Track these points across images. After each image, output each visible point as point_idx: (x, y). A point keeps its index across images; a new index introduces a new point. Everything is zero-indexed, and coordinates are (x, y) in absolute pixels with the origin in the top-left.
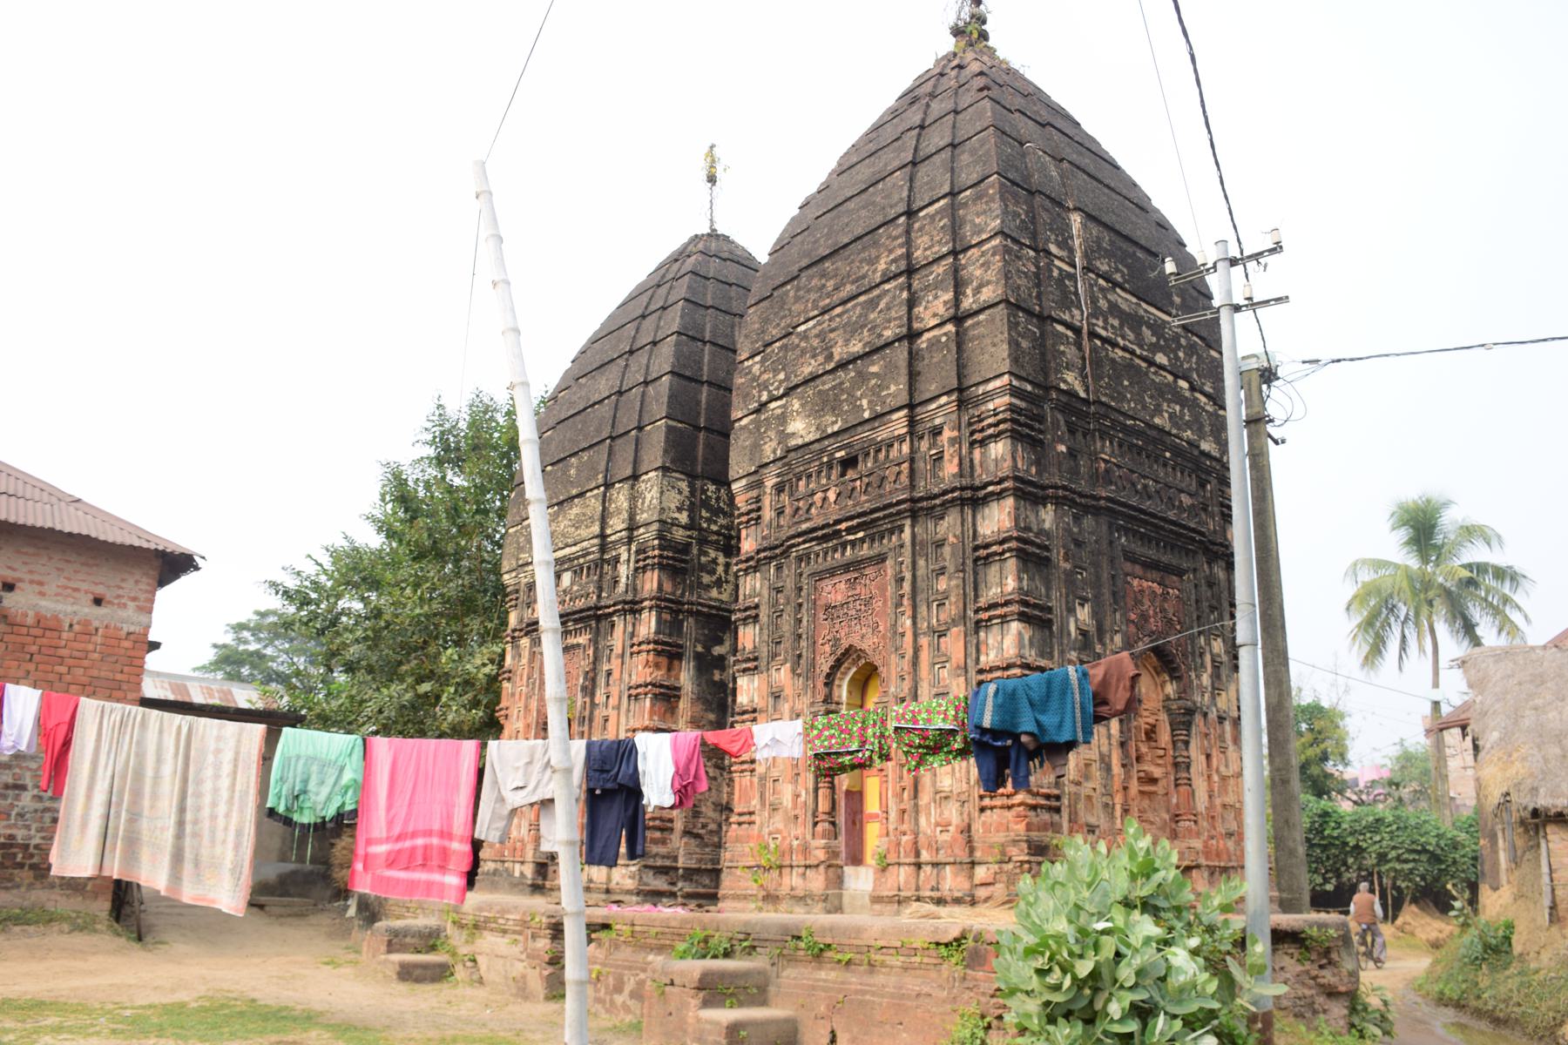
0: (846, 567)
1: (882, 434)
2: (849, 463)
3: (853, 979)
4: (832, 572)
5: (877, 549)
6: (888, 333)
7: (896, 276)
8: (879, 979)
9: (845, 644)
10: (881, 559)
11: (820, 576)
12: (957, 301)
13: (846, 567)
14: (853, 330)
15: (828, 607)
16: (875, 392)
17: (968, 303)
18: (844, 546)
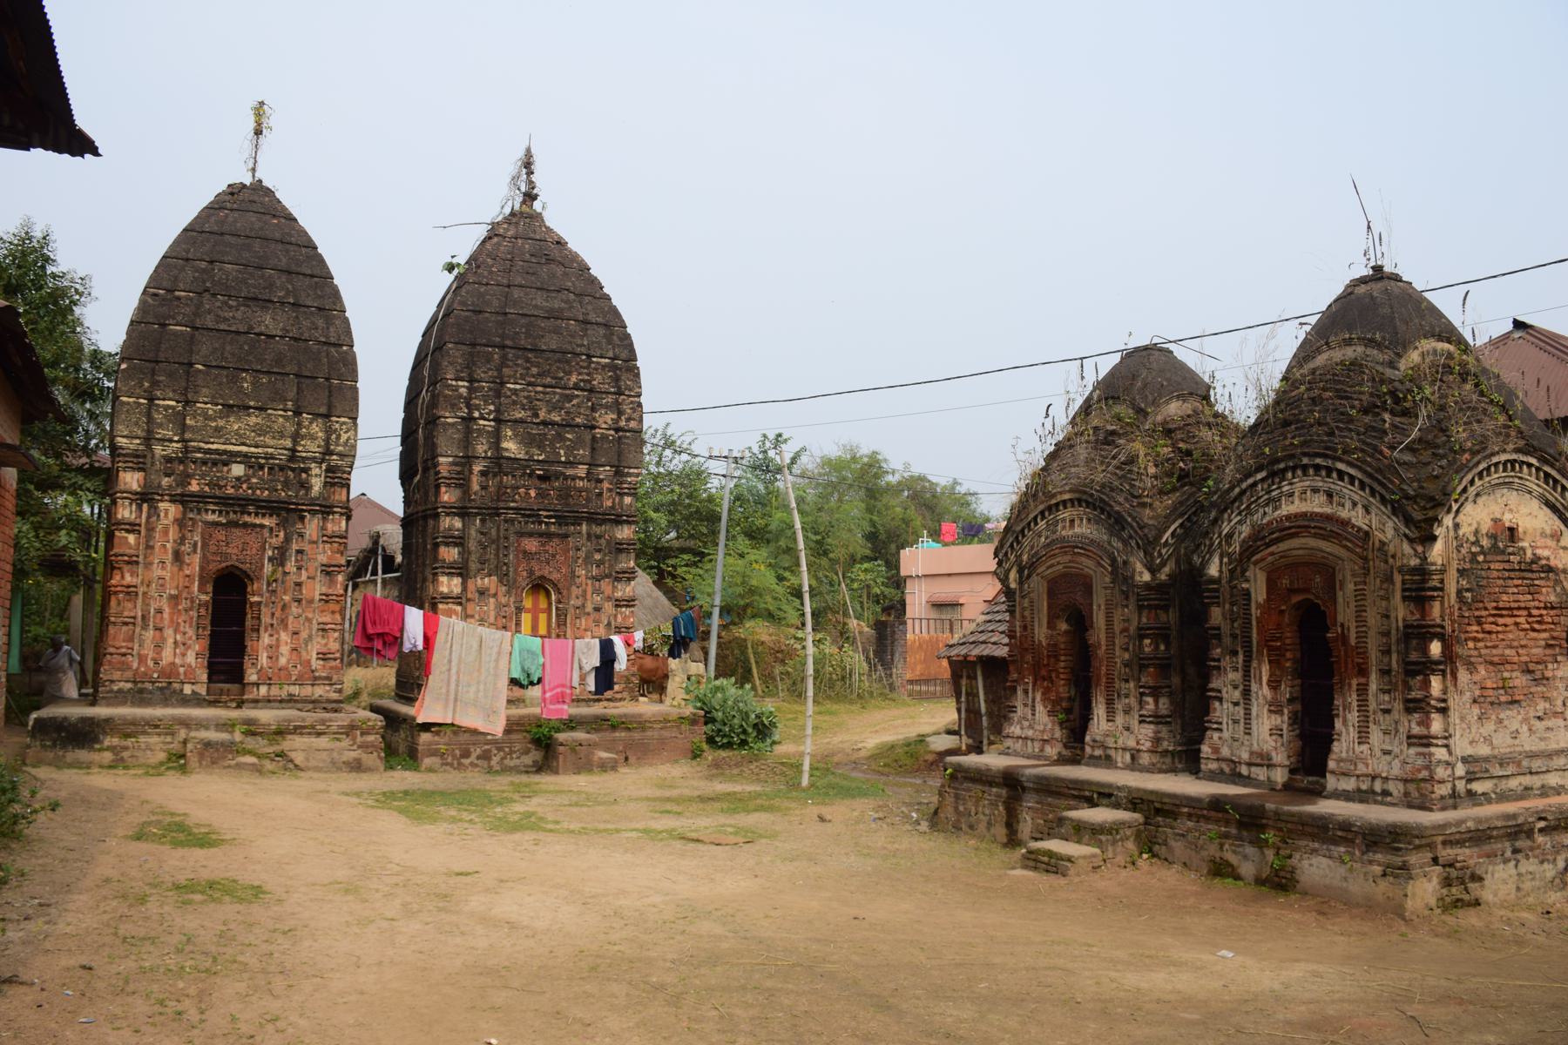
0: (541, 535)
1: (569, 472)
2: (542, 478)
3: (636, 735)
4: (531, 535)
5: (563, 530)
6: (578, 420)
7: (583, 390)
8: (649, 733)
9: (538, 574)
10: (566, 536)
11: (521, 534)
12: (616, 421)
13: (541, 535)
14: (554, 408)
15: (525, 552)
16: (569, 450)
17: (623, 423)
18: (540, 523)
